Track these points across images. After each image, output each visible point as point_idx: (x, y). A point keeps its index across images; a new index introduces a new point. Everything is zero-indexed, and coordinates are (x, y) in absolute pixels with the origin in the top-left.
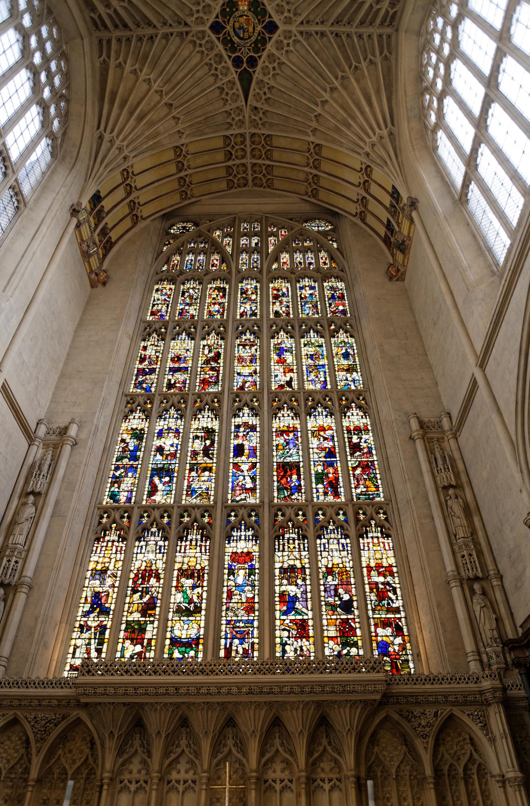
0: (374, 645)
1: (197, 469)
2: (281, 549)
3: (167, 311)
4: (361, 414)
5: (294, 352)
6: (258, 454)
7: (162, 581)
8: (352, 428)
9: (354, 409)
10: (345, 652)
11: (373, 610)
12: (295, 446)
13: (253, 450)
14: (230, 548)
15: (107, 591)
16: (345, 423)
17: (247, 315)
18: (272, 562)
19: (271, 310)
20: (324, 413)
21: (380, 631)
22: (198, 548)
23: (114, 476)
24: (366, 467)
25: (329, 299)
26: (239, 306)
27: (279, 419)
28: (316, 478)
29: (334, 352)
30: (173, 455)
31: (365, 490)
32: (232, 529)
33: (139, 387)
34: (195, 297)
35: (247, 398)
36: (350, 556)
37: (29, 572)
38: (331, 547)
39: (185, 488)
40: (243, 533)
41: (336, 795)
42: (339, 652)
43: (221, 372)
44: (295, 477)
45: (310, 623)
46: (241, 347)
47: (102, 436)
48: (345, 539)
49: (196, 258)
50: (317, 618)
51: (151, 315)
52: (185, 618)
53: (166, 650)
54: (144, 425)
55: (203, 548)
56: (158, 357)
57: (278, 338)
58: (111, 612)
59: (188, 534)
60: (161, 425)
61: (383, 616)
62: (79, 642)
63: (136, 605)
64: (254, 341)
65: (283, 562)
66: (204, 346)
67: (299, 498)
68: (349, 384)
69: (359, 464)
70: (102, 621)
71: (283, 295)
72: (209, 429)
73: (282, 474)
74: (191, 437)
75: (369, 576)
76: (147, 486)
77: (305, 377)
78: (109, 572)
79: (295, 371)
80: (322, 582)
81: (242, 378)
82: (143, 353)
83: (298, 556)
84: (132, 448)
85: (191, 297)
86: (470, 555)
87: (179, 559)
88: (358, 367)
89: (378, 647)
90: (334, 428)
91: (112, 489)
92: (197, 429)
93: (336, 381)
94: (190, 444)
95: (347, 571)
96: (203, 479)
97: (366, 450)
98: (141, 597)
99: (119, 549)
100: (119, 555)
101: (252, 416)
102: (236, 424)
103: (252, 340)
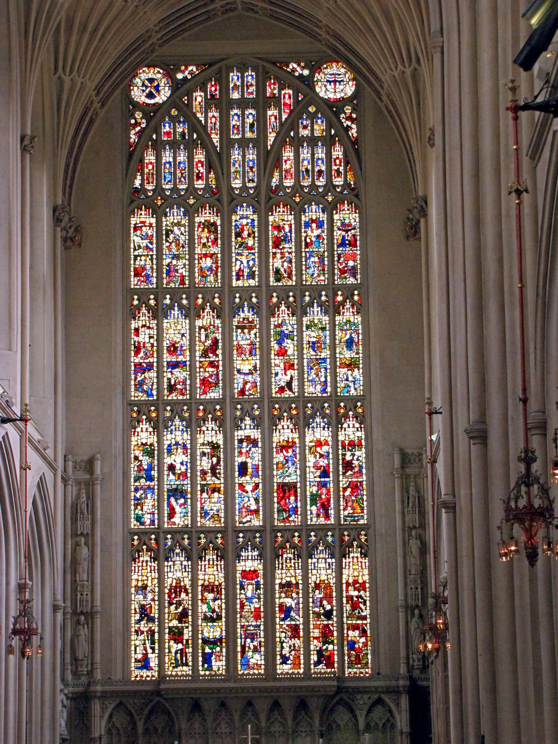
0: (346, 643)
1: (207, 490)
2: (280, 567)
3: (152, 268)
4: (357, 425)
5: (295, 338)
6: (260, 473)
7: (190, 595)
8: (347, 443)
9: (351, 419)
10: (324, 647)
11: (347, 617)
12: (293, 464)
13: (256, 468)
14: (241, 566)
15: (150, 604)
16: (341, 438)
17: (243, 276)
18: (273, 578)
19: (271, 267)
20: (322, 424)
21: (350, 632)
22: (215, 567)
23: (136, 499)
24: (355, 487)
25: (338, 246)
26: (234, 260)
27: (280, 432)
28: (311, 499)
29: (337, 337)
30: (184, 474)
31: (351, 511)
32: (241, 550)
33: (140, 390)
34: (182, 242)
35: (247, 407)
36: (334, 574)
37: (98, 603)
38: (320, 565)
39: (199, 509)
40: (250, 553)
41: (308, 739)
42: (321, 648)
43: (221, 368)
44: (292, 498)
45: (301, 627)
46: (239, 331)
47: (120, 463)
48: (331, 558)
49: (175, 158)
50: (306, 623)
51: (136, 275)
52: (210, 624)
53: (200, 647)
54: (153, 439)
55: (219, 567)
56: (152, 345)
57: (278, 317)
58: (156, 620)
59: (205, 554)
60: (168, 439)
61: (354, 622)
62: (137, 643)
63: (173, 615)
64: (252, 322)
65: (282, 579)
66: (200, 328)
67: (296, 520)
68: (349, 386)
69: (349, 484)
70: (151, 628)
71: (286, 239)
72: (214, 444)
73: (281, 495)
74: (198, 453)
75: (347, 591)
76: (166, 508)
77: (306, 376)
78: (148, 589)
79: (296, 367)
80: (311, 595)
81: (242, 376)
82: (136, 339)
83: (293, 574)
84: (146, 467)
85: (177, 240)
86: (417, 588)
87: (201, 577)
88: (361, 362)
89: (348, 644)
90: (330, 443)
91: (137, 511)
92: (203, 444)
93: (336, 382)
94: (198, 463)
95: (330, 586)
96: (213, 500)
97: (356, 469)
98: (176, 608)
99: (152, 568)
100: (153, 574)
101: (254, 428)
102: (239, 438)
103: (250, 320)
